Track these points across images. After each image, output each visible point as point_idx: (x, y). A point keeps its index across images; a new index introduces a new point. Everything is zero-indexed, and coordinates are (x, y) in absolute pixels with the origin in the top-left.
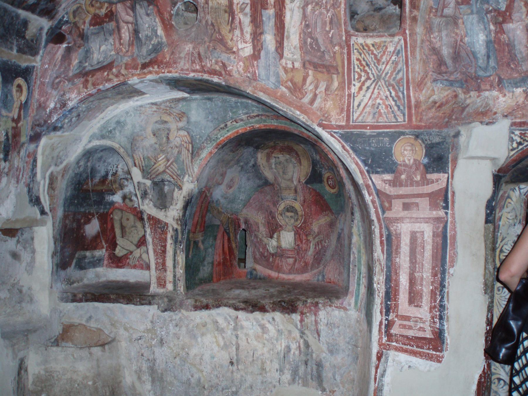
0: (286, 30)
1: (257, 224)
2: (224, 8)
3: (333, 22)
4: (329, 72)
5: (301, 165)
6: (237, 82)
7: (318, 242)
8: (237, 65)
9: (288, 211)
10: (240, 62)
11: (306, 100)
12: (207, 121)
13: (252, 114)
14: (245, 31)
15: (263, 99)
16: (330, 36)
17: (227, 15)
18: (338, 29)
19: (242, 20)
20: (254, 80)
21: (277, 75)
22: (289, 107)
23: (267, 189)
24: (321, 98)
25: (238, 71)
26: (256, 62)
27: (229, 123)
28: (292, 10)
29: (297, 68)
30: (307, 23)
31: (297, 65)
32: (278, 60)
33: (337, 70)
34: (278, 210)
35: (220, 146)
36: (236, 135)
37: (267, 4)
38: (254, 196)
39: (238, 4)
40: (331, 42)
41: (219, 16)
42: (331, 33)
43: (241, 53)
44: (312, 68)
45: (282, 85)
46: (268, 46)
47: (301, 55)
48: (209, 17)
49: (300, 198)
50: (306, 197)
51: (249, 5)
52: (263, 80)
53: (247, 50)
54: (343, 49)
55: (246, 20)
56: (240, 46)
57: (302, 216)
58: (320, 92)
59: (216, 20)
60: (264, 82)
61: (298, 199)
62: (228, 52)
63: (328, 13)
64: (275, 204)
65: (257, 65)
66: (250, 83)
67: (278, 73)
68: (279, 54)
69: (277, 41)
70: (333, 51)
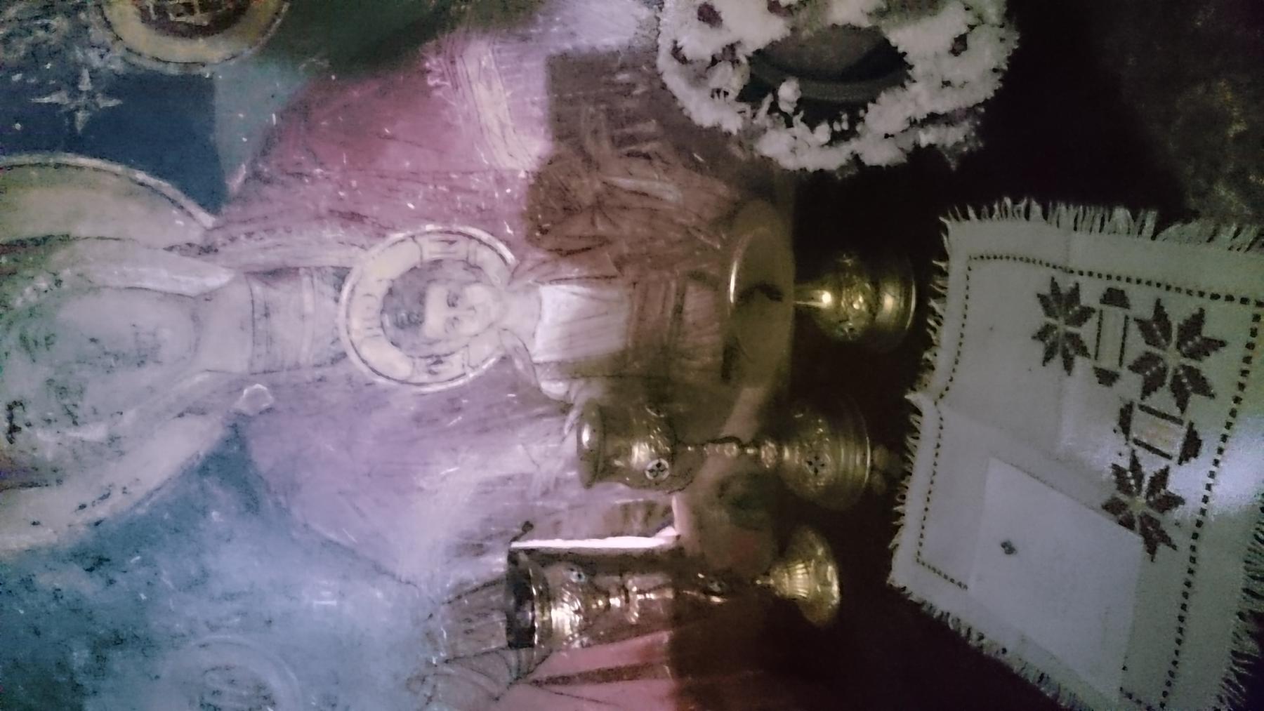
1: (487, 489)
5: (66, 239)
7: (618, 142)
9: (413, 322)
23: (265, 455)
34: (403, 382)
38: (317, 526)
49: (328, 245)
50: (324, 205)
57: (449, 237)
61: (333, 258)
64: (369, 395)
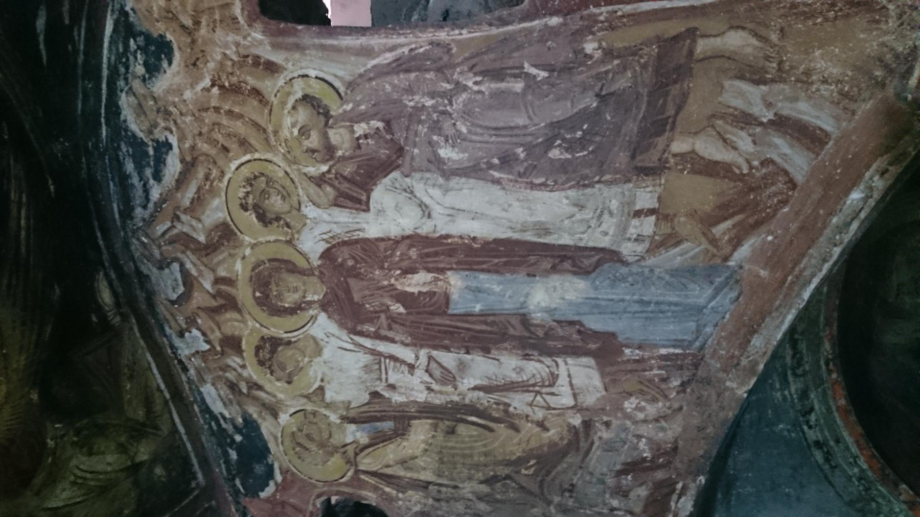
0: (516, 236)
2: (440, 436)
3: (497, 65)
4: (683, 72)
6: (701, 429)
8: (635, 423)
10: (622, 410)
11: (797, 161)
12: (798, 499)
13: (788, 360)
14: (514, 377)
15: (779, 336)
16: (544, 74)
17: (462, 429)
18: (519, 48)
19: (478, 382)
20: (696, 366)
21: (686, 274)
22: (828, 232)
24: (796, 99)
25: (657, 420)
26: (627, 351)
27: (812, 435)
28: (454, 213)
29: (660, 199)
30: (496, 161)
31: (646, 198)
32: (624, 270)
33: (676, 38)
35: (888, 471)
36: (853, 418)
37: (432, 294)
39: (429, 389)
40: (567, 69)
41: (464, 456)
42: (534, 71)
43: (590, 400)
44: (661, 141)
45: (726, 259)
46: (570, 303)
47: (609, 183)
48: (468, 489)
51: (435, 353)
52: (698, 331)
53: (580, 378)
54: (593, 19)
55: (481, 369)
56: (567, 400)
58: (769, 105)
59: (476, 466)
60: (708, 329)
62: (583, 445)
63: (465, 88)
65: (640, 347)
66: (707, 381)
67: (675, 273)
68: (598, 264)
69: (554, 269)
70: (602, 61)
